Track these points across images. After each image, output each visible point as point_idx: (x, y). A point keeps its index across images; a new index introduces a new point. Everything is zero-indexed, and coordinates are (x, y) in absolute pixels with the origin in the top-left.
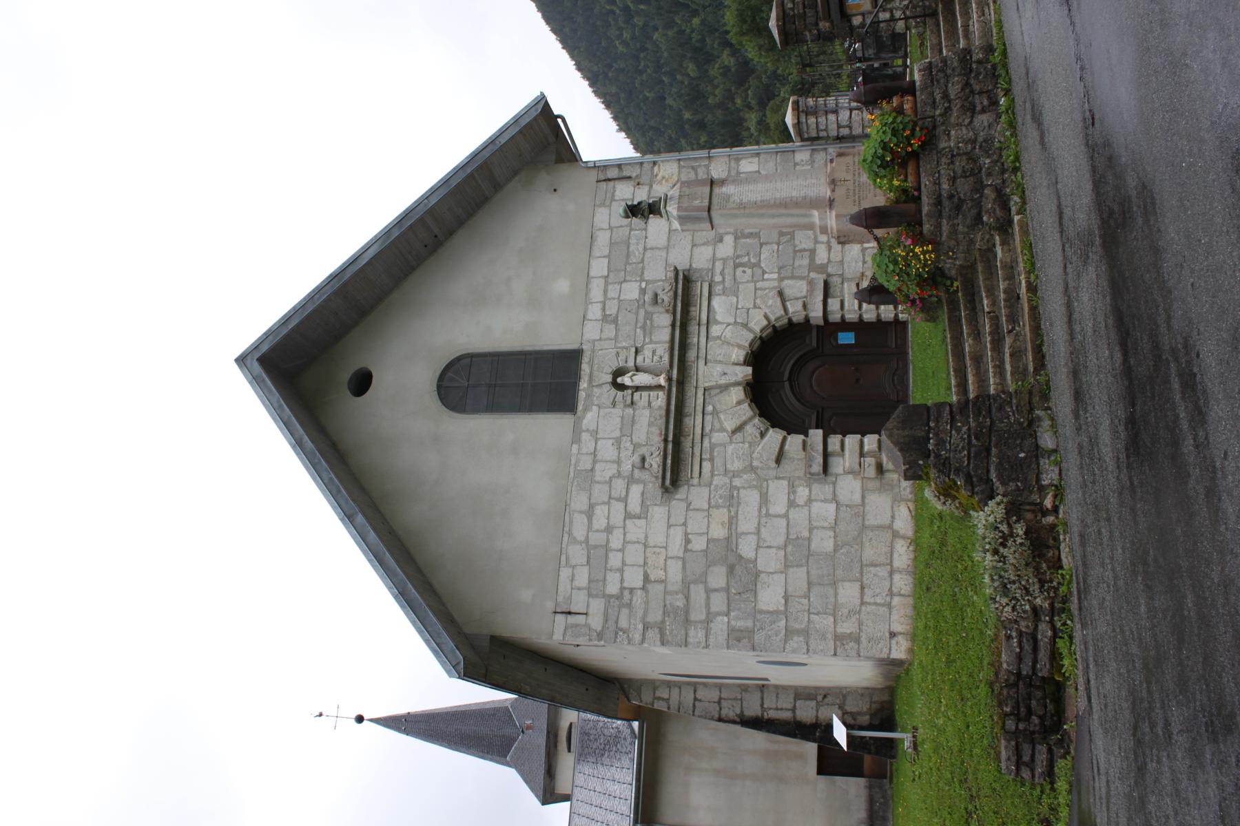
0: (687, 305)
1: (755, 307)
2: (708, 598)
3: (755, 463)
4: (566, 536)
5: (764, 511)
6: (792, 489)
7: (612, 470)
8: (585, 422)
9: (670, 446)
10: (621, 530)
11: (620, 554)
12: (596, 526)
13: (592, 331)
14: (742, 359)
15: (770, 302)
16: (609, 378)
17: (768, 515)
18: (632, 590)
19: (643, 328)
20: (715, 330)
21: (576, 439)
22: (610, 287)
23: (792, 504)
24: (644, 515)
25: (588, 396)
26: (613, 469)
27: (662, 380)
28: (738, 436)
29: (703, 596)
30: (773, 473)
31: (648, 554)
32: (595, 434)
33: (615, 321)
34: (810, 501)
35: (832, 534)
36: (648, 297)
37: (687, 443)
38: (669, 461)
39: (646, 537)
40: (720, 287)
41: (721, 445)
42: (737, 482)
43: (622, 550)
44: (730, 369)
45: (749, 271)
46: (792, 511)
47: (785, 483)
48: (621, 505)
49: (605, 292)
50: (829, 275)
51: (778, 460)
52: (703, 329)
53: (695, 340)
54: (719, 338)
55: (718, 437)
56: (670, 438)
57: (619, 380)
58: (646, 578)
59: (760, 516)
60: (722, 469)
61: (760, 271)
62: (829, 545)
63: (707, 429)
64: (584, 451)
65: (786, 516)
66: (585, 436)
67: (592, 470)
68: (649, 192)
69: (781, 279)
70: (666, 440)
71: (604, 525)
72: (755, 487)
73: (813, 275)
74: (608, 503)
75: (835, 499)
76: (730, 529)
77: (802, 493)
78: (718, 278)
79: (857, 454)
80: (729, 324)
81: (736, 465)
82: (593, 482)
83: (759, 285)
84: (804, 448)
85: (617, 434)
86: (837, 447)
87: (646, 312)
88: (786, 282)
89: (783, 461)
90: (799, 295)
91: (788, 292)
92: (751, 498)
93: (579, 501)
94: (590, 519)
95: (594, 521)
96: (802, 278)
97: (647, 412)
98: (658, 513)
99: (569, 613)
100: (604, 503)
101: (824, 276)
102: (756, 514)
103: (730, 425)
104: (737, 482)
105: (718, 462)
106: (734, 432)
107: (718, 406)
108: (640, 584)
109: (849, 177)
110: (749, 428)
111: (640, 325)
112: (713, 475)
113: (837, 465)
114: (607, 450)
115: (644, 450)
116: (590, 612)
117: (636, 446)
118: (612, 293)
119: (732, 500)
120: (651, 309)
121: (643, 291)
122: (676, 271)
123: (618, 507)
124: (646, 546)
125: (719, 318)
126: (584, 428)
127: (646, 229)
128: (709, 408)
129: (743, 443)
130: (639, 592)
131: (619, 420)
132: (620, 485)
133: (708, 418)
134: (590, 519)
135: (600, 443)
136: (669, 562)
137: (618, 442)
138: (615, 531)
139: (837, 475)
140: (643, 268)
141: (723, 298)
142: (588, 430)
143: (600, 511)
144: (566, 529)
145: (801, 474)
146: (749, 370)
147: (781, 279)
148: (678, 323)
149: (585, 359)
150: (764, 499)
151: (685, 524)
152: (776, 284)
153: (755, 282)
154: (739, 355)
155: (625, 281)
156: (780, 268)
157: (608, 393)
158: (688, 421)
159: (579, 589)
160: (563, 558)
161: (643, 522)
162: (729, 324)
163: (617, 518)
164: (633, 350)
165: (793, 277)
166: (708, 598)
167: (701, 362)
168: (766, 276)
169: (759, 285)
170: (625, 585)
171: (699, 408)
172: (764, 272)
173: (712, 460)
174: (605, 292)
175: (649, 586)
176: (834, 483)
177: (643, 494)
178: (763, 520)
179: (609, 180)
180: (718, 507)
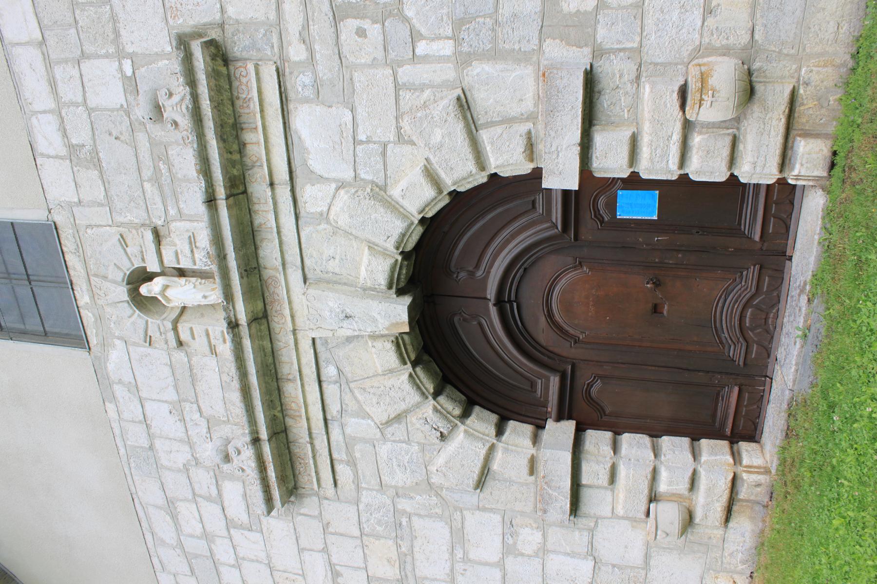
0: (232, 131)
1: (400, 138)
3: (435, 480)
4: (149, 537)
5: (459, 554)
6: (509, 526)
7: (182, 456)
8: (111, 366)
9: (267, 449)
12: (187, 529)
15: (437, 136)
16: (122, 292)
17: (466, 559)
19: (156, 179)
20: (313, 197)
21: (107, 395)
22: (58, 72)
23: (509, 550)
25: (99, 318)
28: (398, 431)
30: (472, 498)
32: (135, 388)
33: (95, 162)
34: (543, 551)
36: (142, 111)
37: (298, 430)
40: (306, 79)
41: (365, 441)
42: (404, 504)
44: (358, 306)
45: (374, 30)
46: (510, 561)
47: (497, 518)
48: (216, 509)
49: (53, 84)
50: (599, 52)
51: (480, 484)
52: (283, 193)
54: (324, 217)
55: (355, 426)
56: (264, 435)
57: (144, 290)
60: (374, 482)
61: (403, 32)
63: (333, 409)
64: (126, 415)
65: (501, 565)
66: (119, 390)
67: (151, 447)
69: (463, 60)
70: (256, 441)
72: (440, 517)
73: (554, 50)
75: (592, 553)
76: (402, 567)
77: (529, 538)
78: (296, 52)
80: (342, 185)
81: (400, 478)
82: (158, 466)
83: (406, 73)
84: (532, 471)
85: (171, 395)
86: (604, 479)
87: (152, 143)
88: (479, 69)
89: (490, 483)
90: (515, 110)
91: (484, 101)
92: (433, 536)
93: (149, 493)
94: (174, 517)
96: (521, 57)
97: (211, 362)
98: (277, 525)
101: (581, 58)
102: (447, 556)
103: (381, 414)
104: (404, 504)
105: (366, 469)
106: (389, 422)
107: (347, 369)
110: (413, 419)
111: (147, 173)
112: (358, 488)
113: (596, 500)
114: (164, 421)
115: (226, 431)
117: (211, 423)
118: (70, 92)
119: (399, 527)
120: (156, 130)
121: (131, 84)
122: (183, 42)
125: (316, 164)
126: (113, 377)
128: (329, 371)
129: (408, 442)
131: (167, 371)
132: (203, 479)
133: (330, 390)
134: (174, 517)
137: (177, 409)
138: (219, 541)
139: (597, 519)
140: (114, 19)
141: (319, 109)
142: (120, 382)
143: (186, 510)
144: (145, 524)
145: (529, 508)
147: (463, 60)
148: (221, 193)
150: (458, 537)
151: (325, 550)
152: (448, 72)
153: (395, 66)
154: (377, 269)
155: (84, 56)
156: (459, 24)
157: (133, 320)
158: (292, 391)
160: (155, 561)
162: (342, 185)
164: (149, 236)
165: (495, 54)
167: (295, 276)
168: (422, 48)
169: (406, 73)
172: (415, 36)
173: (352, 463)
174: (53, 84)
176: (592, 531)
177: (245, 495)
178: (459, 567)
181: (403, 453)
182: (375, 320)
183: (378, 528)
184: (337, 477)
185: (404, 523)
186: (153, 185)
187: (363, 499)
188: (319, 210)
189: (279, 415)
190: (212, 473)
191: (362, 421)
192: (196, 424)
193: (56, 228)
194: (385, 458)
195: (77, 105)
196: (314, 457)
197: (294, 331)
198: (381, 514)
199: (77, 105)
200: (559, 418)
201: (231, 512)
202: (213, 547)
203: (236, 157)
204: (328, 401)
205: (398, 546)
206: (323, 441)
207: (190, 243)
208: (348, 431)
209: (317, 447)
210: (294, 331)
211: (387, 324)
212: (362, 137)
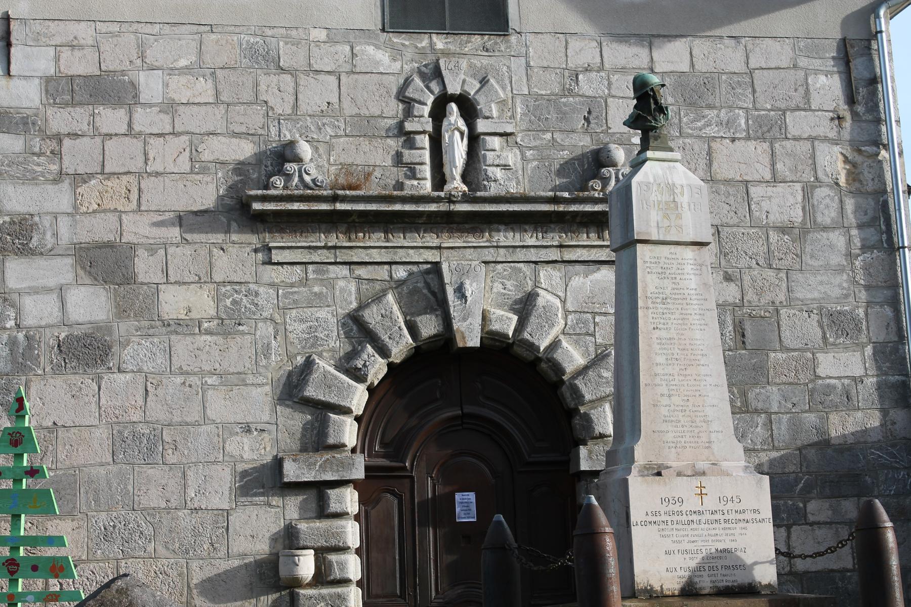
2: (48, 290)
8: (370, 49)
9: (324, 207)
10: (168, 129)
11: (123, 129)
12: (177, 82)
13: (541, 50)
14: (496, 327)
18: (57, 154)
24: (198, 167)
26: (283, 107)
27: (457, 185)
29: (52, 282)
31: (125, 178)
35: (173, 504)
38: (296, 206)
39: (157, 174)
43: (130, 132)
52: (554, 255)
53: (531, 241)
56: (340, 206)
57: (454, 106)
58: (80, 179)
59: (202, 373)
62: (153, 499)
63: (362, 272)
68: (826, 139)
71: (176, 97)
74: (218, 101)
79: (322, 543)
95: (183, 80)
99: (9, 45)
100: (217, 94)
108: (69, 165)
109: (710, 503)
116: (15, 82)
123: (214, 119)
124: (140, 175)
125: (577, 281)
127: (748, 138)
130: (55, 168)
135: (332, 79)
136: (112, 218)
138: (167, 119)
146: (474, 341)
148: (561, 208)
149: (489, 41)
159: (57, 59)
161: (184, 164)
163: (189, 120)
164: (509, 129)
166: (48, 290)
170: (67, 142)
171: (401, 256)
175: (66, 185)
178: (195, 380)
179: (847, 63)
180: (218, 299)
181: (326, 333)
182: (464, 319)
183: (228, 302)
184: (285, 266)
185: (241, 328)
186: (549, 141)
187: (262, 290)
188: (542, 281)
189: (350, 220)
190: (260, 132)
191: (353, 297)
192: (320, 129)
193: (504, 35)
194: (318, 315)
195: (609, 88)
196: (309, 248)
197: (439, 248)
198: (248, 306)
199: (609, 88)
200: (368, 469)
201: (214, 141)
202: (156, 109)
203: (578, 219)
204: (370, 267)
205: (210, 320)
206: (328, 258)
207: (505, 166)
208: (341, 283)
209: (320, 252)
210: (439, 248)
211: (463, 329)
212: (597, 319)
